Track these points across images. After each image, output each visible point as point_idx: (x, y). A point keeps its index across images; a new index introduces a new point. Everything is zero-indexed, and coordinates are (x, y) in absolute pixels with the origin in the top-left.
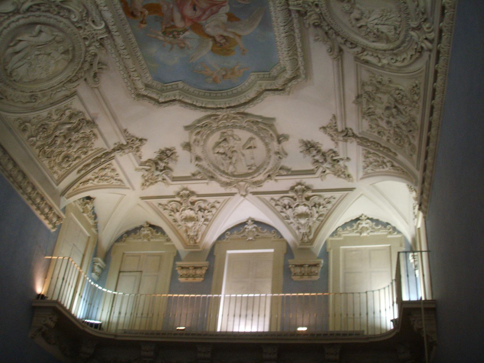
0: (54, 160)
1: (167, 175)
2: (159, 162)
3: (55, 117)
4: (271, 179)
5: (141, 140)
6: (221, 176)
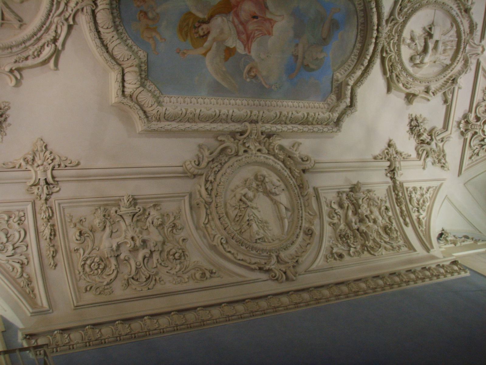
0: (385, 242)
1: (438, 135)
2: (421, 138)
3: (336, 221)
4: (470, 9)
5: (389, 145)
6: (453, 69)
